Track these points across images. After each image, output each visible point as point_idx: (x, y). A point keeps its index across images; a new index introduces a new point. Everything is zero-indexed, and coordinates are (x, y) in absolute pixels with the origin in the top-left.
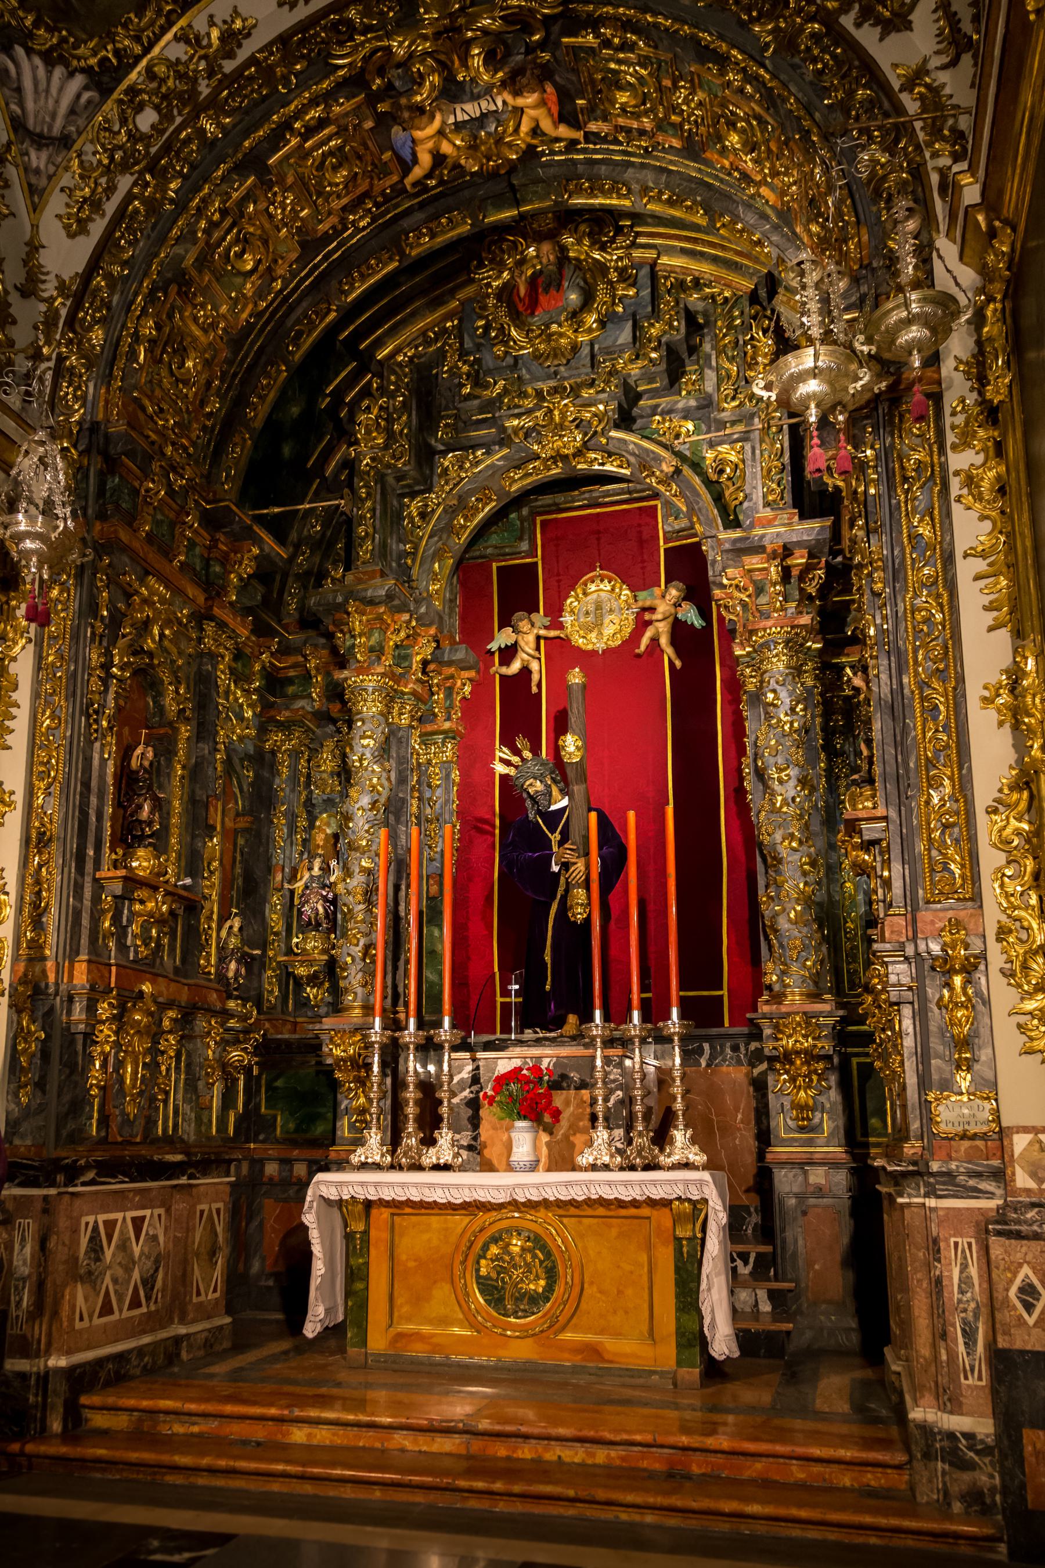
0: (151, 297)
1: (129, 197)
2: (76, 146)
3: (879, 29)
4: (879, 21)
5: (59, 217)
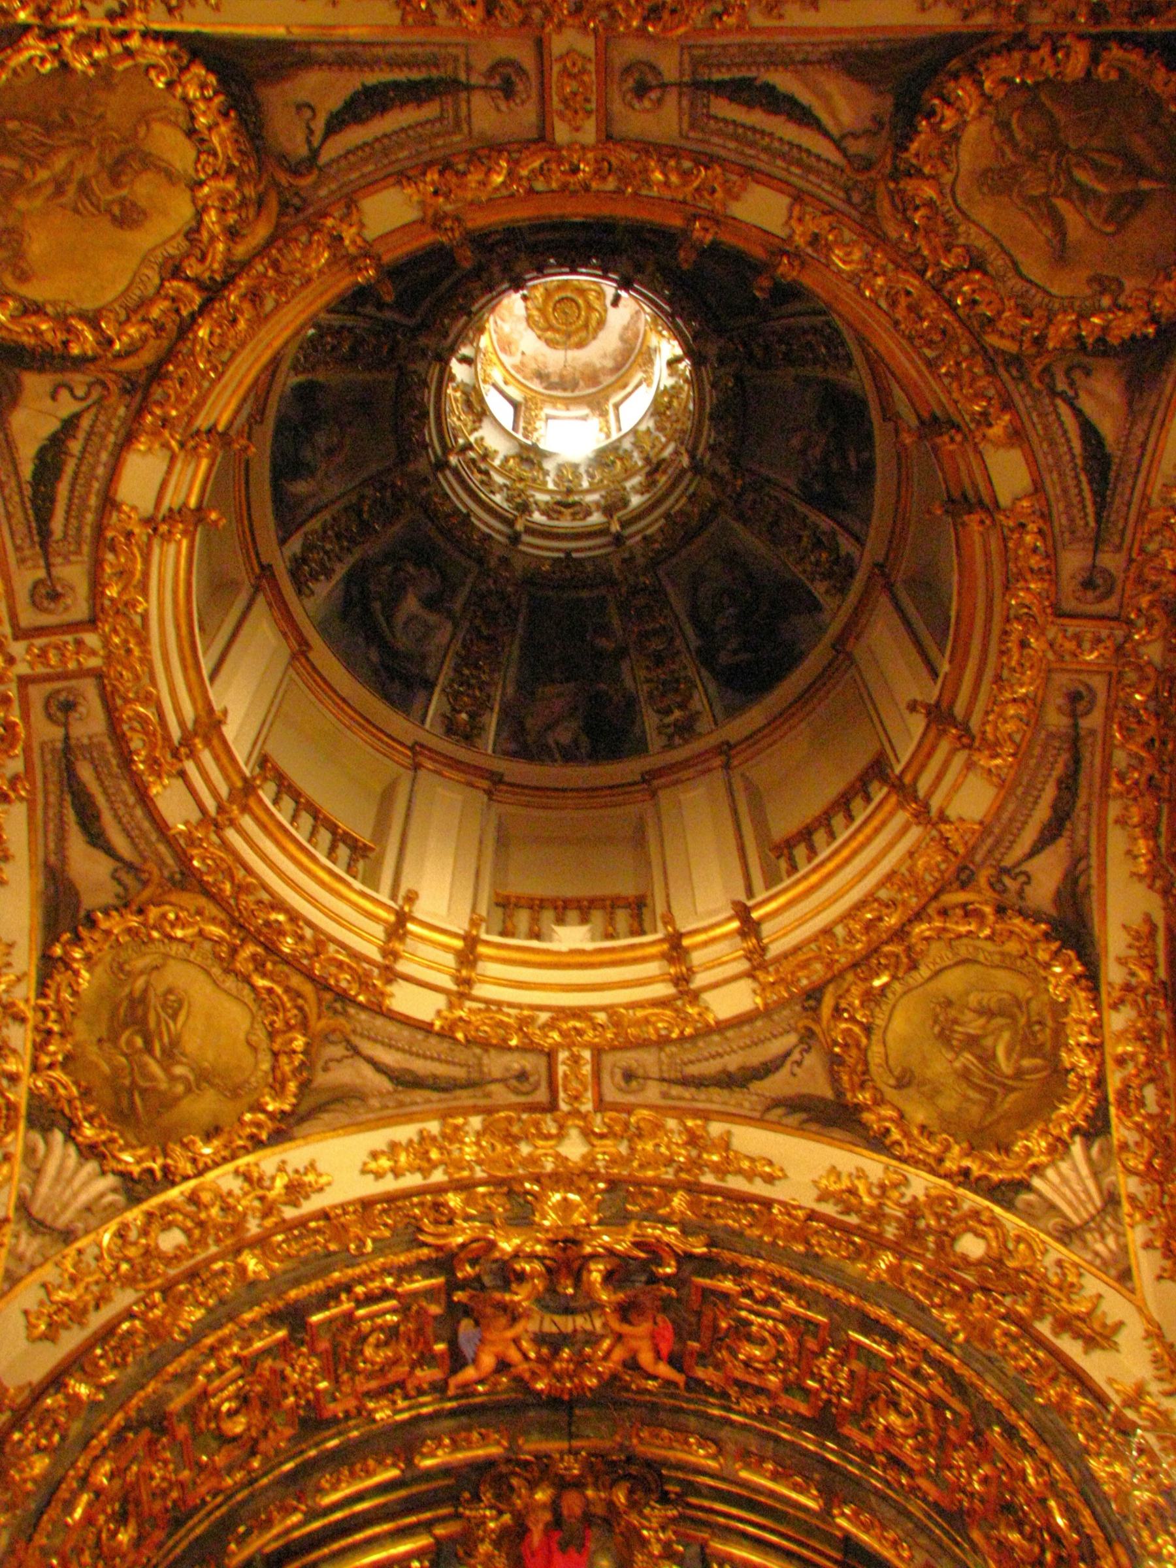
0: (119, 1438)
4: (1077, 1335)
5: (26, 1313)
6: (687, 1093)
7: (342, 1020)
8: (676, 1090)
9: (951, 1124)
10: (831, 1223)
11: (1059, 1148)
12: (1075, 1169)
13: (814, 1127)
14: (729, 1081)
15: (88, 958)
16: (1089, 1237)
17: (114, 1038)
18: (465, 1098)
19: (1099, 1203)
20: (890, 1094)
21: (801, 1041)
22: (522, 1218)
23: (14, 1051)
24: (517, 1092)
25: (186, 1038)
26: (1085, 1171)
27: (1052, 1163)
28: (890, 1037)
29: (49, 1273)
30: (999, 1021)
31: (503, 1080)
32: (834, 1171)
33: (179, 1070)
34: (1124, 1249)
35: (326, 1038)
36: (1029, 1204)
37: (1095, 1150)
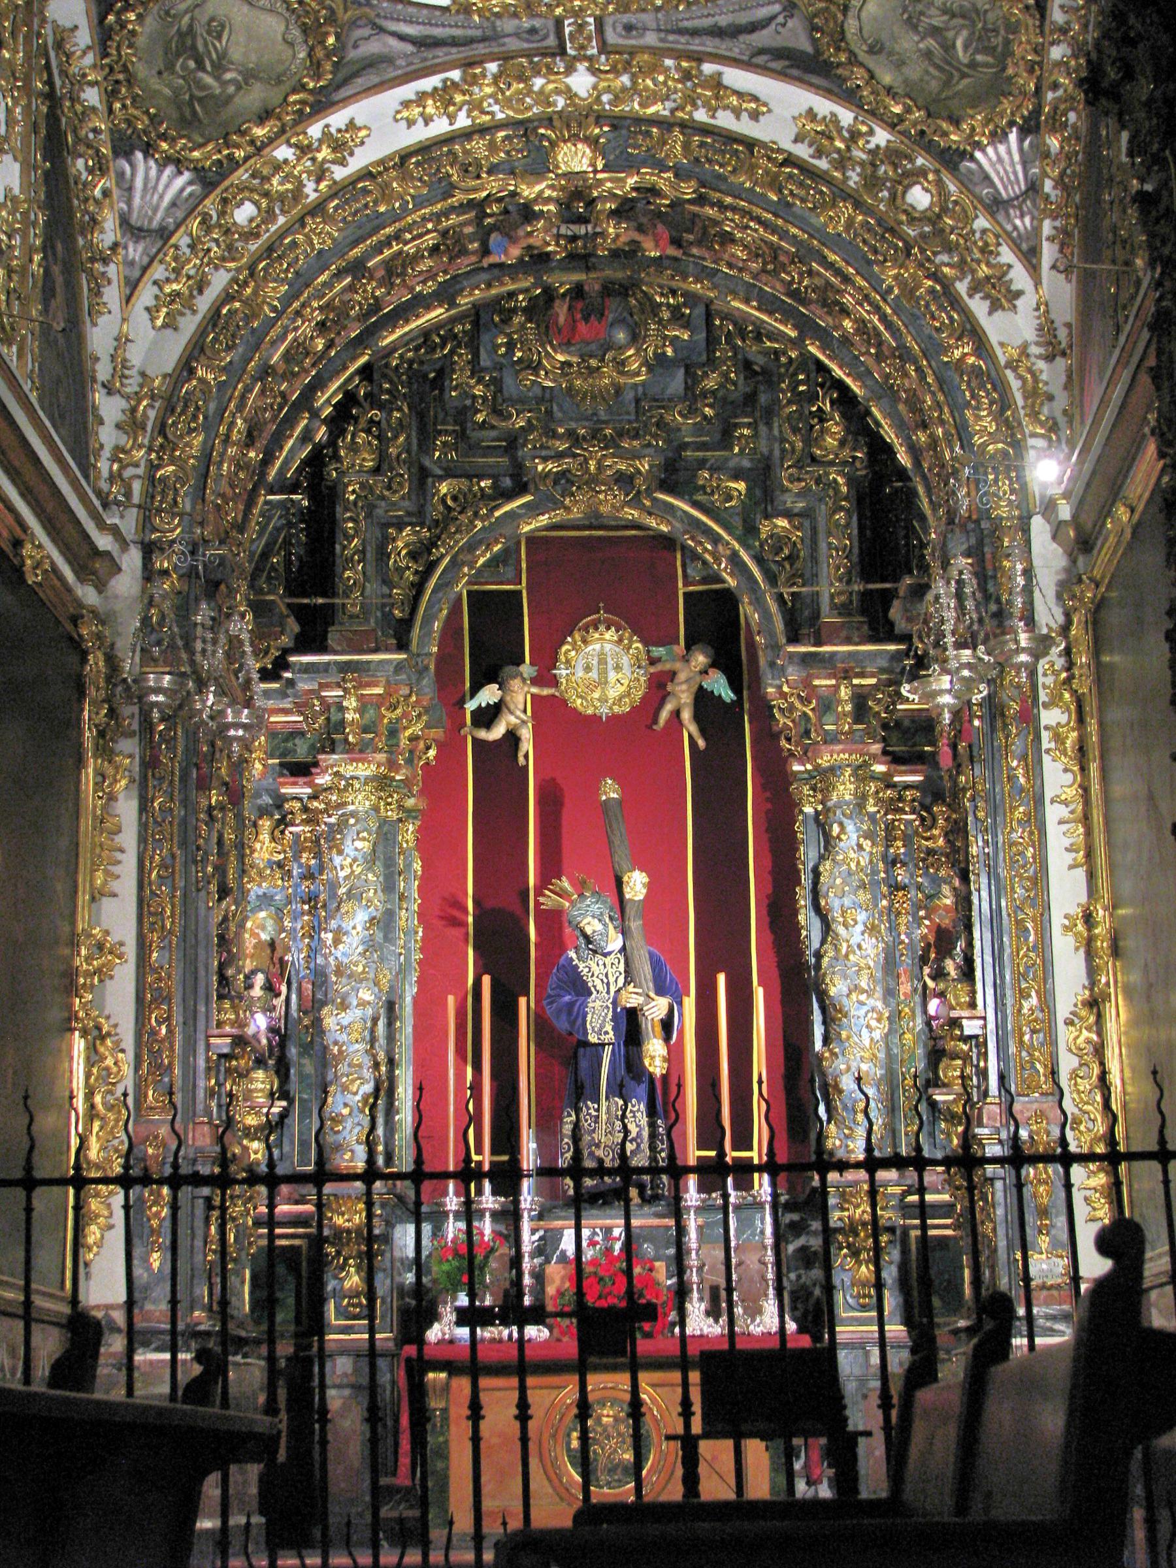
1: (228, 298)
2: (173, 241)
3: (987, 303)
4: (986, 297)
5: (147, 309)
6: (683, 40)
7: (367, 10)
8: (671, 38)
9: (911, 93)
10: (806, 169)
11: (998, 136)
12: (1009, 152)
13: (795, 72)
14: (718, 32)
15: (140, 17)
16: (1011, 211)
17: (170, 67)
18: (481, 49)
19: (1023, 187)
20: (862, 56)
21: (784, 9)
22: (539, 165)
23: (94, 109)
24: (528, 41)
25: (231, 50)
26: (1016, 157)
27: (992, 143)
28: (864, 14)
29: (158, 272)
30: (958, 21)
31: (516, 35)
32: (811, 114)
33: (228, 76)
34: (1037, 230)
35: (354, 24)
36: (969, 170)
37: (1027, 143)
